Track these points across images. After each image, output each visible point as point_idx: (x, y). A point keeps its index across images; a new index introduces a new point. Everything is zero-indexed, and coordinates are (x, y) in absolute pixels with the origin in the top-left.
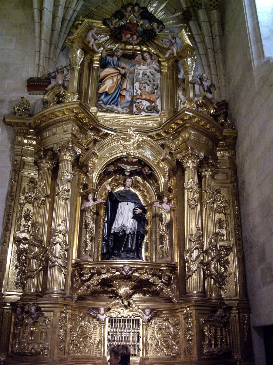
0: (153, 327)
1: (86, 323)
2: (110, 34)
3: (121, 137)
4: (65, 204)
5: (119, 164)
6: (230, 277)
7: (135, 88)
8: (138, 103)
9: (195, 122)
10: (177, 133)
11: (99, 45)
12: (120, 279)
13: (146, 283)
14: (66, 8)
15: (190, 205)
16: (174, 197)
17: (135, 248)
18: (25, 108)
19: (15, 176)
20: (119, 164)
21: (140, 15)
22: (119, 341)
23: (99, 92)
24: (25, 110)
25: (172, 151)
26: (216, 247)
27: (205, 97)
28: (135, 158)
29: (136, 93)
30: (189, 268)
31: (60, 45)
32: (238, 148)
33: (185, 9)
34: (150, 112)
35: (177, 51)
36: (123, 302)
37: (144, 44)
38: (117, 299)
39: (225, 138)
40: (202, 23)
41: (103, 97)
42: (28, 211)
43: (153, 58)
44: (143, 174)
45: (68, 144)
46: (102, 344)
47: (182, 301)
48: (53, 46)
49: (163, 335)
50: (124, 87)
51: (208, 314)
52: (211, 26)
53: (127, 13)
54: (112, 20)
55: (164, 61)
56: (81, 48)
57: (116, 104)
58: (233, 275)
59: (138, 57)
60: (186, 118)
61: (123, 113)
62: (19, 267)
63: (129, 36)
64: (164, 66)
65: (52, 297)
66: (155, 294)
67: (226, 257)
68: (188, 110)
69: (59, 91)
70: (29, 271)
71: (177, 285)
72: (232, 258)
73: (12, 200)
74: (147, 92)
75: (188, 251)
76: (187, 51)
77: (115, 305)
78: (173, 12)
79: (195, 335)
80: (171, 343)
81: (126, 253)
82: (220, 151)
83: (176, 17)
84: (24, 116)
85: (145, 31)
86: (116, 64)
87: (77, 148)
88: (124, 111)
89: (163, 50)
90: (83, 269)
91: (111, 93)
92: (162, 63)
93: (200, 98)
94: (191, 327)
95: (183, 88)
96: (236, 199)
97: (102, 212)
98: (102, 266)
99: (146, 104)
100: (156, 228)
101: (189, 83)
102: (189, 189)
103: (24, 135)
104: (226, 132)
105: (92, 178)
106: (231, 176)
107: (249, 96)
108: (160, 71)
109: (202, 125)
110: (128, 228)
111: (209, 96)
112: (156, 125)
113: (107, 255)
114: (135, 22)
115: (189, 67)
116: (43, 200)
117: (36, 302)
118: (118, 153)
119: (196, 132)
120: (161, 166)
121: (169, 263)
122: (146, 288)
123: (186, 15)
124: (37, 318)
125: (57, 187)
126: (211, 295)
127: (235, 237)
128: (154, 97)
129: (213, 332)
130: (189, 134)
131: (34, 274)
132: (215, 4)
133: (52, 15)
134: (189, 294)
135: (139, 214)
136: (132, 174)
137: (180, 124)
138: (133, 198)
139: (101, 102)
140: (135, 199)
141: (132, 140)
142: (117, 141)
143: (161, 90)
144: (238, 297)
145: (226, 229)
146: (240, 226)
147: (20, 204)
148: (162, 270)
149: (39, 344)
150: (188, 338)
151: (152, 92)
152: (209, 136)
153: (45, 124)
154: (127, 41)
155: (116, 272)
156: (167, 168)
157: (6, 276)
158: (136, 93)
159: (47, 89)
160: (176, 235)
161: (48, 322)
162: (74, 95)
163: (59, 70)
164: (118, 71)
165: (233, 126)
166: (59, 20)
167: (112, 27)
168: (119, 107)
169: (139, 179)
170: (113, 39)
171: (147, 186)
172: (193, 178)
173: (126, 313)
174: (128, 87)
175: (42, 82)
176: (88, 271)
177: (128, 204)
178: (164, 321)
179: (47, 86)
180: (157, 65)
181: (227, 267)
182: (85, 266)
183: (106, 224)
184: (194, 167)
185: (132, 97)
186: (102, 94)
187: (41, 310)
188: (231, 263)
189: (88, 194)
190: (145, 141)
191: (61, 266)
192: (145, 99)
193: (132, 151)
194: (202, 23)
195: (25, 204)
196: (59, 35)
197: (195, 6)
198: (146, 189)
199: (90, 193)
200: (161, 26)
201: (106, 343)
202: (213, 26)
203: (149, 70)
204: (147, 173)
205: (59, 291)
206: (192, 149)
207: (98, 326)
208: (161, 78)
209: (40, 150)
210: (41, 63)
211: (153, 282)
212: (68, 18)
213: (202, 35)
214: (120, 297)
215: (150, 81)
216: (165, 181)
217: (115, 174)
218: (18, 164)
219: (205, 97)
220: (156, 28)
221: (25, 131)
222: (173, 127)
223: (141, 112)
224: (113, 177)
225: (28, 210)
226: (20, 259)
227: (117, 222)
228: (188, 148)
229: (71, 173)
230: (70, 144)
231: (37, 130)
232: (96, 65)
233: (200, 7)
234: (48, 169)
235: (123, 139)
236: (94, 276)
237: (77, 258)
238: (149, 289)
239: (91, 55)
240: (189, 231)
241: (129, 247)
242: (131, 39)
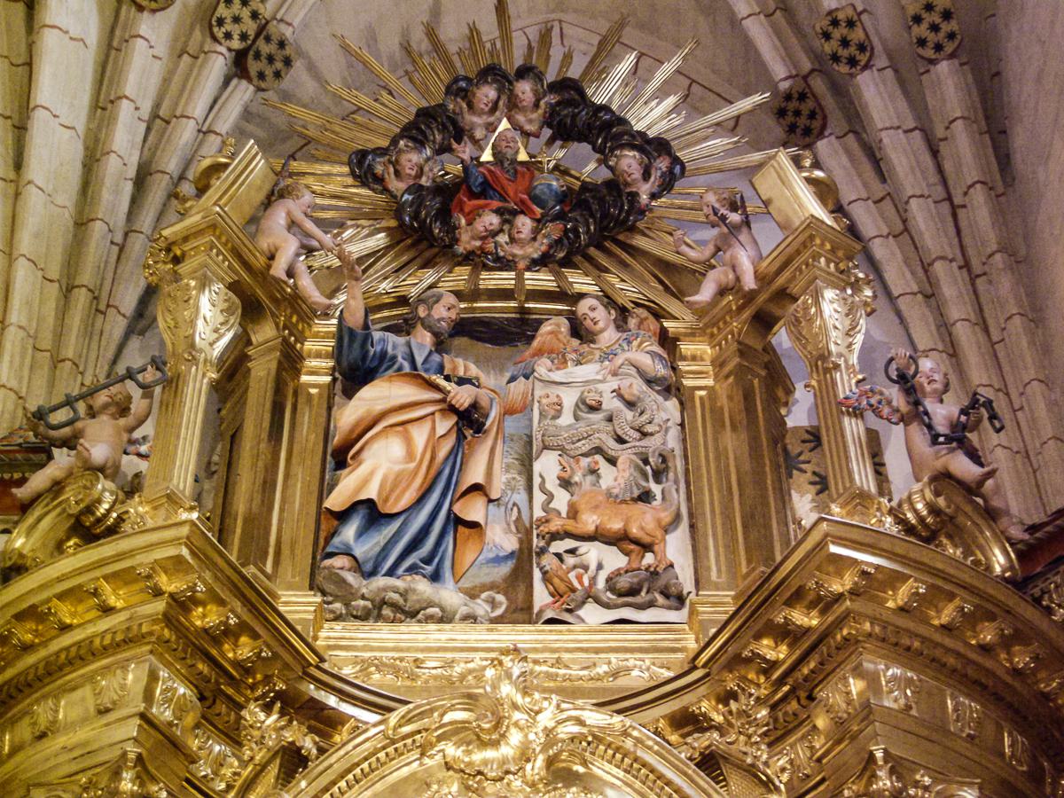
2: (393, 223)
3: (447, 719)
7: (537, 481)
8: (558, 556)
11: (335, 279)
14: (159, 122)
21: (548, 122)
33: (784, 86)
34: (630, 599)
37: (578, 259)
40: (883, 134)
41: (349, 532)
43: (632, 322)
45: (116, 775)
48: (81, 298)
50: (475, 474)
52: (935, 153)
53: (481, 113)
54: (400, 152)
55: (692, 334)
56: (222, 280)
57: (429, 569)
59: (545, 328)
60: (836, 587)
61: (471, 618)
68: (842, 532)
74: (609, 494)
85: (578, 200)
89: (676, 278)
91: (395, 510)
92: (686, 348)
95: (814, 473)
108: (670, 388)
109: (946, 628)
114: (523, 156)
115: (834, 334)
119: (912, 669)
130: (872, 680)
132: (942, 35)
139: (339, 562)
141: (513, 730)
143: (688, 483)
151: (636, 493)
152: (998, 698)
158: (545, 508)
164: (438, 396)
167: (397, 186)
170: (413, 245)
180: (653, 354)
185: (525, 533)
186: (343, 516)
190: (597, 738)
194: (883, 134)
196: (122, 248)
197: (835, 58)
200: (662, 164)
202: (944, 149)
203: (614, 383)
208: (682, 425)
212: (172, 164)
213: (893, 200)
215: (621, 440)
220: (637, 175)
222: (771, 655)
228: (871, 756)
230: (127, 775)
232: (316, 374)
233: (863, 58)
235: (457, 732)
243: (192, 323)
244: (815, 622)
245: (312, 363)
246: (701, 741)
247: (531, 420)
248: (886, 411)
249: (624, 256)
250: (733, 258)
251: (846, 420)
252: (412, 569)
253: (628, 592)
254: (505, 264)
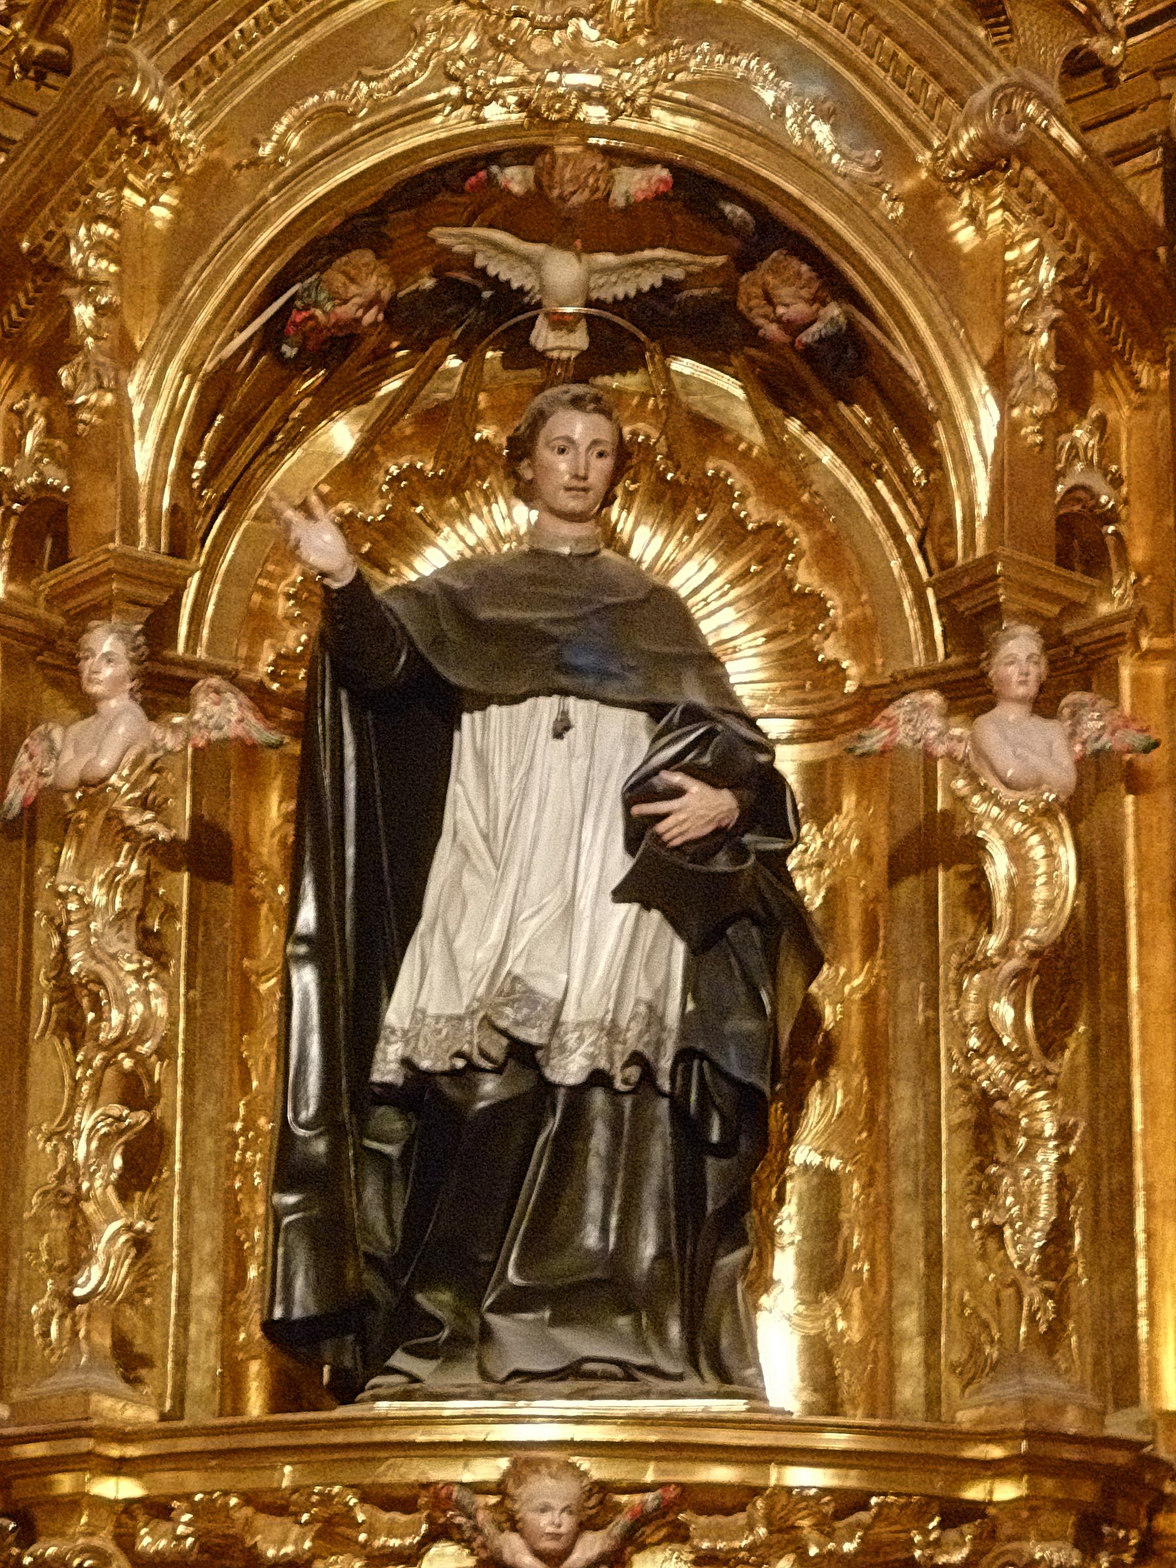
5: (443, 236)
16: (1142, 618)
17: (662, 1254)
20: (443, 236)
25: (1098, 44)
28: (641, 161)
44: (752, 334)
90: (42, 1521)
98: (251, 1481)
110: (570, 1014)
113: (328, 1349)
118: (425, 112)
120: (965, 236)
121: (1071, 1422)
148: (975, 1511)
155: (430, 1539)
176: (104, 1541)
177: (561, 729)
182: (65, 1483)
183: (305, 979)
198: (810, 517)
199: (100, 611)
204: (794, 328)
216: (1009, 430)
217: (419, 345)
224: (392, 385)
227: (437, 945)
241: (591, 1238)
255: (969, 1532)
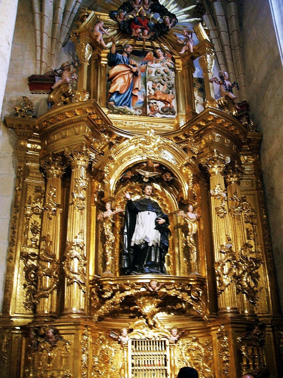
0: (180, 349)
1: (107, 346)
2: (118, 28)
3: (140, 139)
4: (81, 213)
6: (261, 291)
7: (147, 87)
9: (220, 124)
10: (199, 136)
12: (145, 296)
13: (175, 300)
15: (218, 214)
18: (28, 108)
19: (19, 184)
21: (150, 8)
22: (145, 365)
23: (110, 91)
24: (28, 111)
25: (195, 155)
26: (247, 259)
27: (227, 97)
29: (149, 93)
30: (221, 282)
31: (62, 40)
32: (264, 152)
35: (193, 47)
36: (147, 322)
38: (141, 319)
39: (249, 141)
41: (114, 97)
42: (35, 223)
43: (166, 54)
44: (163, 180)
46: (126, 369)
47: (213, 319)
48: (55, 40)
49: (193, 357)
51: (244, 332)
52: (227, 21)
55: (178, 58)
57: (128, 104)
58: (264, 290)
59: (149, 54)
60: (209, 119)
62: (28, 286)
63: (140, 30)
64: (178, 64)
65: (72, 318)
66: (180, 312)
67: (256, 271)
69: (67, 90)
70: (41, 290)
71: (206, 301)
72: (261, 271)
73: (17, 211)
75: (219, 264)
76: (206, 47)
77: (138, 325)
78: (183, 6)
79: (233, 355)
80: (203, 366)
81: (149, 268)
82: (244, 155)
83: (187, 11)
84: (27, 117)
86: (127, 61)
87: (91, 152)
88: (137, 113)
89: (177, 46)
92: (177, 61)
93: (222, 98)
94: (228, 347)
96: (264, 208)
97: (118, 223)
98: (125, 282)
99: (161, 105)
100: (179, 240)
101: (209, 82)
102: (216, 196)
103: (27, 138)
104: (250, 135)
105: (109, 185)
106: (257, 183)
107: (278, 95)
108: (174, 70)
109: (226, 127)
111: (232, 95)
112: (172, 128)
114: (145, 15)
116: (54, 211)
117: (53, 324)
120: (184, 171)
122: (171, 306)
123: (200, 8)
124: (56, 342)
125: (71, 196)
126: (243, 312)
127: (264, 248)
128: (170, 97)
129: (250, 351)
130: (214, 136)
131: (47, 293)
133: (52, 6)
134: (223, 311)
135: (162, 224)
136: (151, 180)
137: (202, 126)
138: (155, 207)
140: (156, 208)
142: (136, 144)
144: (271, 314)
145: (254, 240)
146: (270, 236)
147: (27, 215)
149: (59, 371)
150: (224, 359)
153: (51, 126)
154: (137, 37)
156: (191, 174)
157: (13, 296)
159: (53, 87)
160: (202, 246)
161: (68, 347)
162: (84, 94)
163: (65, 67)
165: (257, 127)
166: (61, 11)
167: (120, 20)
168: (132, 108)
169: (157, 186)
171: (167, 194)
172: (219, 184)
173: (151, 334)
174: (140, 86)
175: (46, 80)
177: (149, 213)
178: (193, 341)
179: (53, 85)
181: (257, 281)
182: (104, 282)
184: (221, 173)
185: (145, 97)
186: (112, 94)
187: (59, 332)
188: (261, 276)
189: (104, 203)
191: (81, 283)
192: (161, 100)
193: (153, 155)
195: (31, 215)
199: (108, 201)
200: (174, 20)
201: (130, 368)
202: (229, 22)
203: (163, 68)
204: (167, 179)
205: (79, 311)
206: (218, 153)
207: (119, 349)
209: (49, 155)
210: (44, 60)
211: (183, 298)
214: (145, 316)
215: (164, 81)
218: (21, 171)
219: (227, 97)
220: (169, 22)
221: (28, 135)
222: (195, 129)
223: (156, 113)
225: (35, 222)
226: (28, 278)
228: (214, 151)
229: (86, 180)
230: (84, 147)
231: (42, 134)
232: (104, 62)
234: (58, 176)
236: (117, 293)
237: (95, 274)
238: (174, 307)
239: (99, 51)
240: (219, 241)
242: (141, 34)
243: (84, 53)
244: (204, 125)
245: (103, 59)
246: (183, 145)
247: (146, 74)
248: (217, 82)
249: (165, 39)
250: (189, 45)
251: (210, 83)
252: (125, 104)
253: (164, 111)
254: (142, 40)
255: (190, 287)
